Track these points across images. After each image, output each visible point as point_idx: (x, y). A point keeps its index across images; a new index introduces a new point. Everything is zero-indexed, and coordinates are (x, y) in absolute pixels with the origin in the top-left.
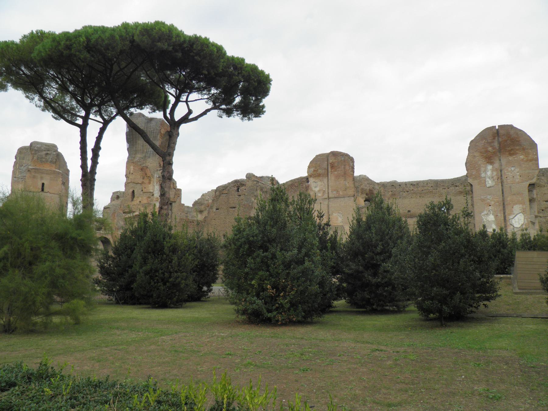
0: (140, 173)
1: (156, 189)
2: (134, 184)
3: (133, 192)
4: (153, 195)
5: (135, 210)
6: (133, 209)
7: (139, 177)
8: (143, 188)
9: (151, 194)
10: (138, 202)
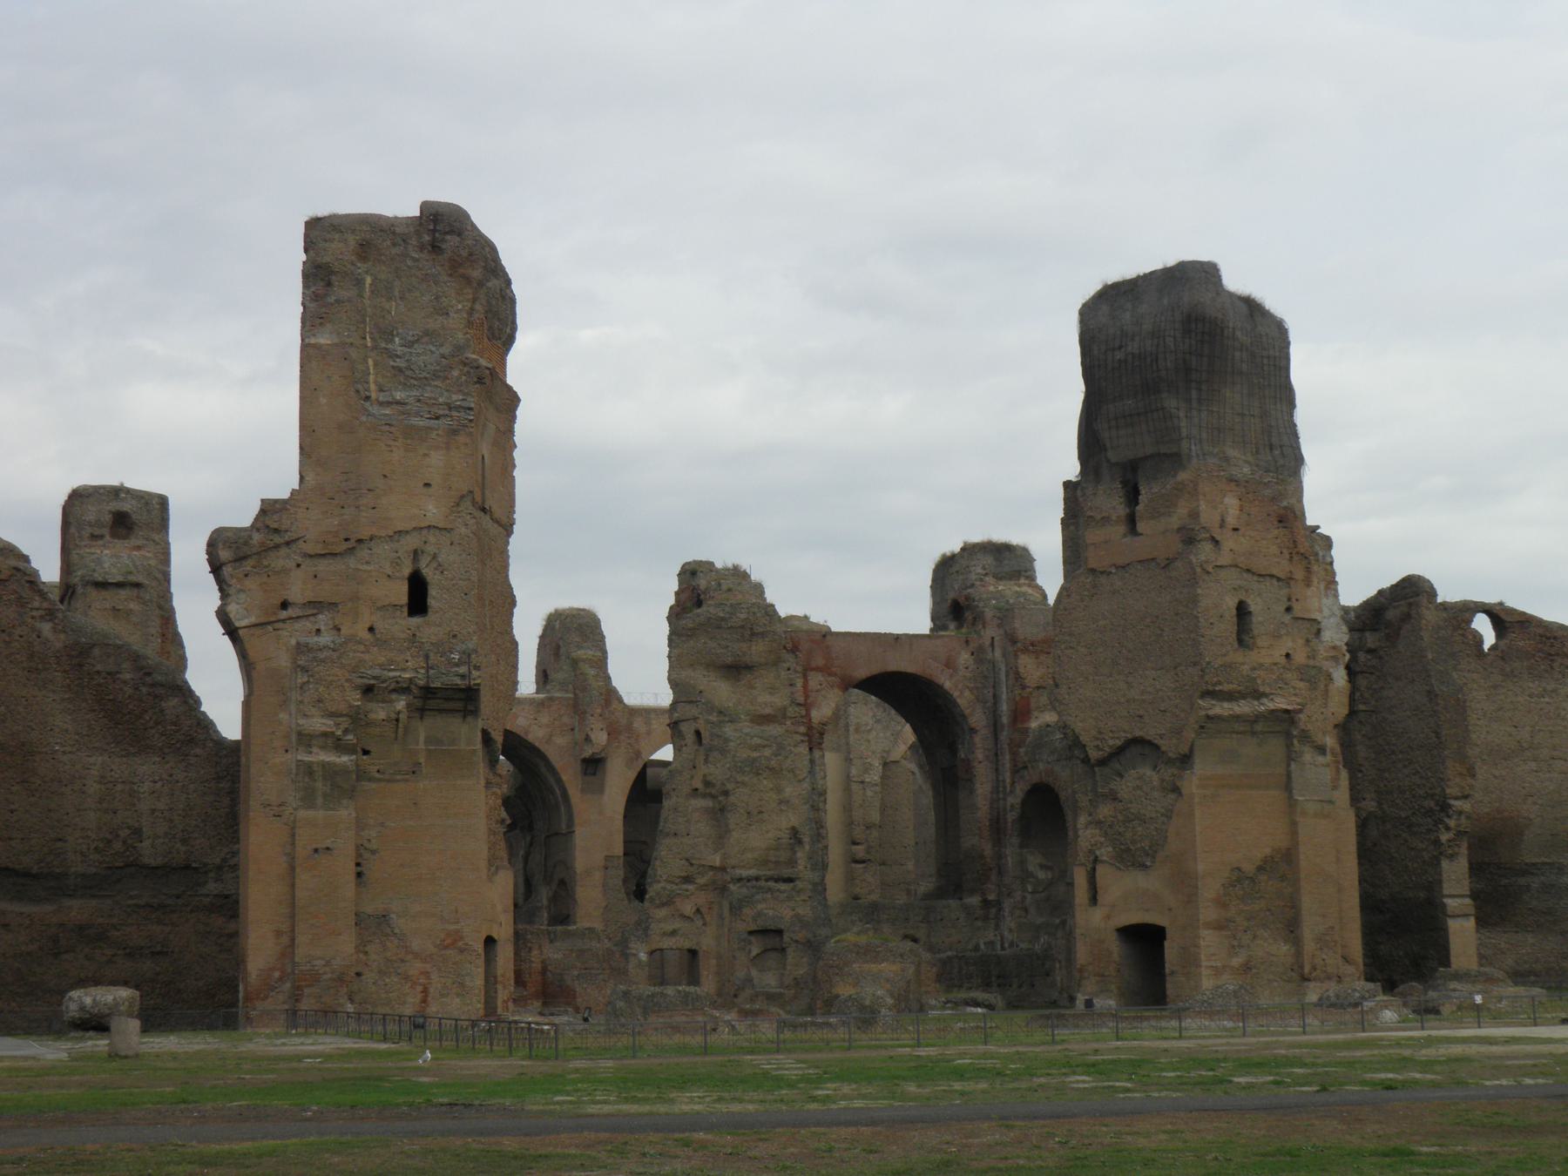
0: (1276, 532)
1: (1326, 612)
2: (1245, 575)
3: (1242, 611)
4: (1319, 632)
5: (1267, 690)
6: (1259, 681)
7: (1274, 549)
8: (1294, 600)
9: (1314, 630)
10: (1278, 655)
